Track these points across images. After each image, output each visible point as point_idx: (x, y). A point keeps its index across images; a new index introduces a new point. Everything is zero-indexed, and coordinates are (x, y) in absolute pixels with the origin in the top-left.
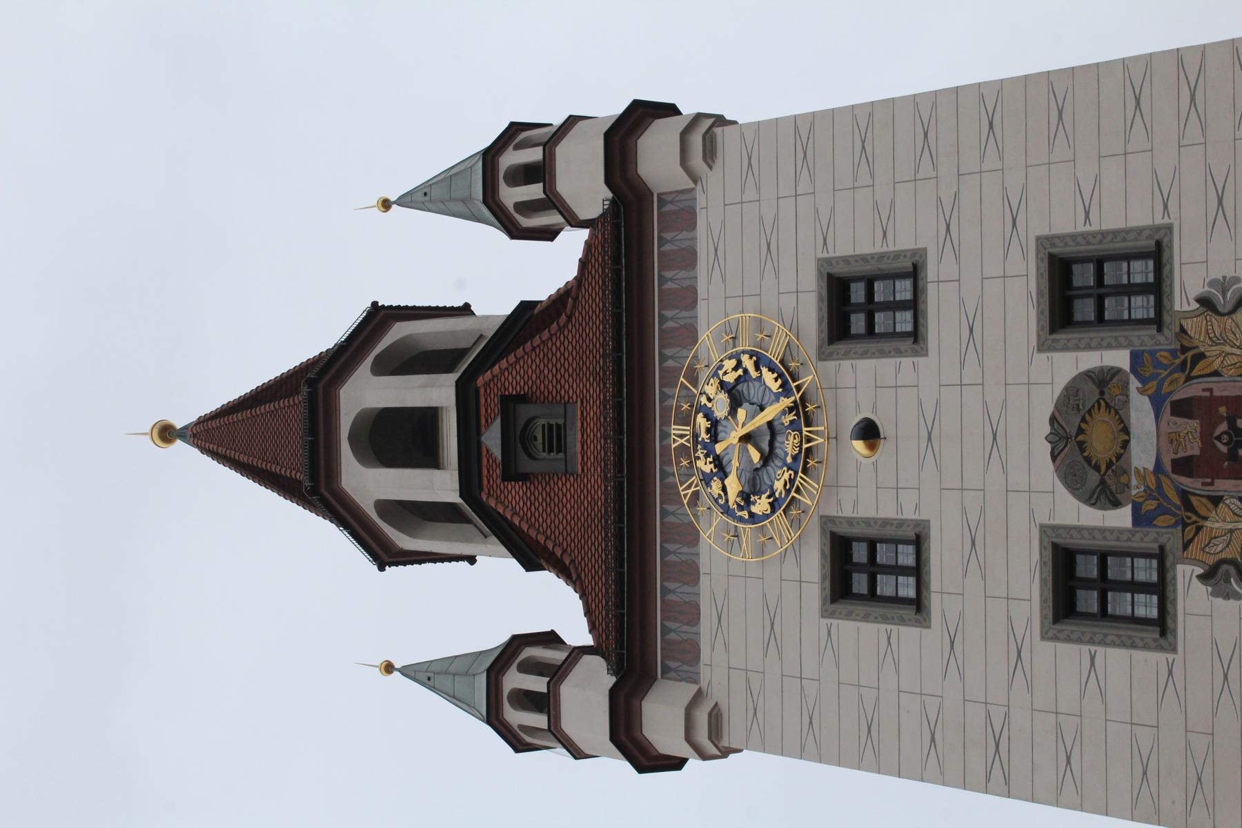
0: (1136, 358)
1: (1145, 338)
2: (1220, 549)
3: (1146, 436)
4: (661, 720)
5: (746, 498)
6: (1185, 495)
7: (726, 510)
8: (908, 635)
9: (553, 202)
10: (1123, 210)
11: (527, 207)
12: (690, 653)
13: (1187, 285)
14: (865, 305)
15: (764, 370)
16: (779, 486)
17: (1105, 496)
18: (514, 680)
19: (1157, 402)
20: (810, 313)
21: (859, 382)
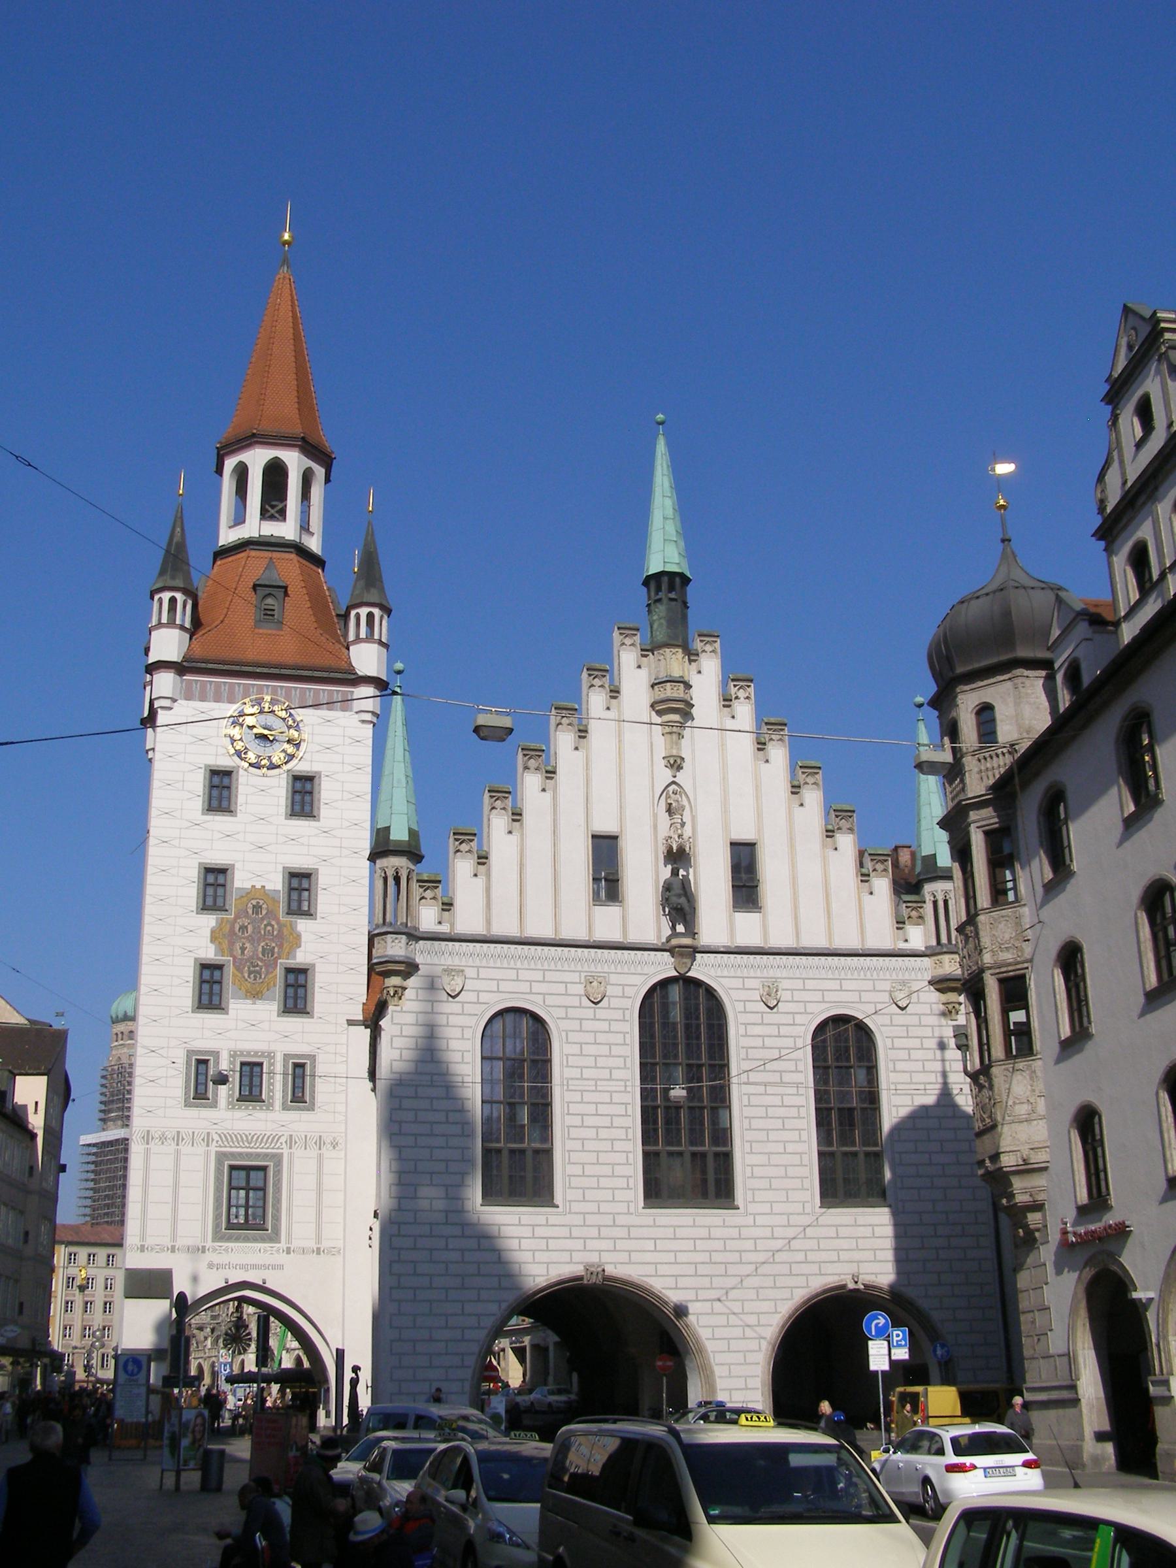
4: (164, 682)
8: (198, 803)
9: (358, 640)
11: (358, 616)
12: (189, 697)
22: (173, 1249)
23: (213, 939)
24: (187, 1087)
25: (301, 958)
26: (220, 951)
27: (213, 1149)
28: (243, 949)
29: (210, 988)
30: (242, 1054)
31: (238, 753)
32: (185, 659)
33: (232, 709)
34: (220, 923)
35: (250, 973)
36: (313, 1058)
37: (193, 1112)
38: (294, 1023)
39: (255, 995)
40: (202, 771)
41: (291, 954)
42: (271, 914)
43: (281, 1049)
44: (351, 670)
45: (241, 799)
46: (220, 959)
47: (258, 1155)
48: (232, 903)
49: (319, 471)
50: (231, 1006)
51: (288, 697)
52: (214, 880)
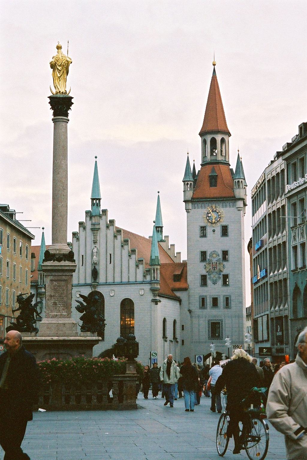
0: (220, 259)
1: (222, 259)
2: (207, 266)
3: (214, 260)
5: (208, 216)
6: (210, 263)
7: (207, 213)
8: (198, 236)
10: (230, 257)
11: (235, 181)
12: (194, 208)
13: (225, 263)
14: (225, 231)
15: (219, 219)
16: (210, 220)
17: (210, 256)
18: (189, 183)
19: (217, 261)
20: (224, 224)
21: (219, 230)
22: (199, 342)
25: (225, 272)
27: (207, 319)
29: (204, 280)
32: (192, 198)
33: (205, 211)
37: (201, 310)
38: (225, 288)
44: (235, 197)
47: (217, 320)
49: (226, 137)
51: (219, 205)
52: (203, 254)
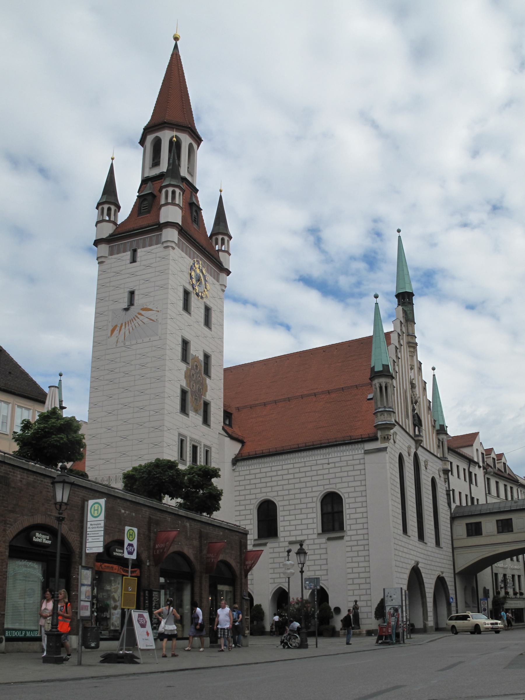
23: (185, 377)
24: (178, 453)
26: (187, 384)
28: (193, 386)
30: (193, 441)
31: (193, 285)
34: (187, 368)
35: (195, 399)
36: (210, 448)
39: (196, 411)
40: (182, 287)
41: (205, 395)
42: (200, 372)
43: (205, 441)
45: (192, 309)
46: (187, 388)
48: (190, 360)
50: (190, 414)
